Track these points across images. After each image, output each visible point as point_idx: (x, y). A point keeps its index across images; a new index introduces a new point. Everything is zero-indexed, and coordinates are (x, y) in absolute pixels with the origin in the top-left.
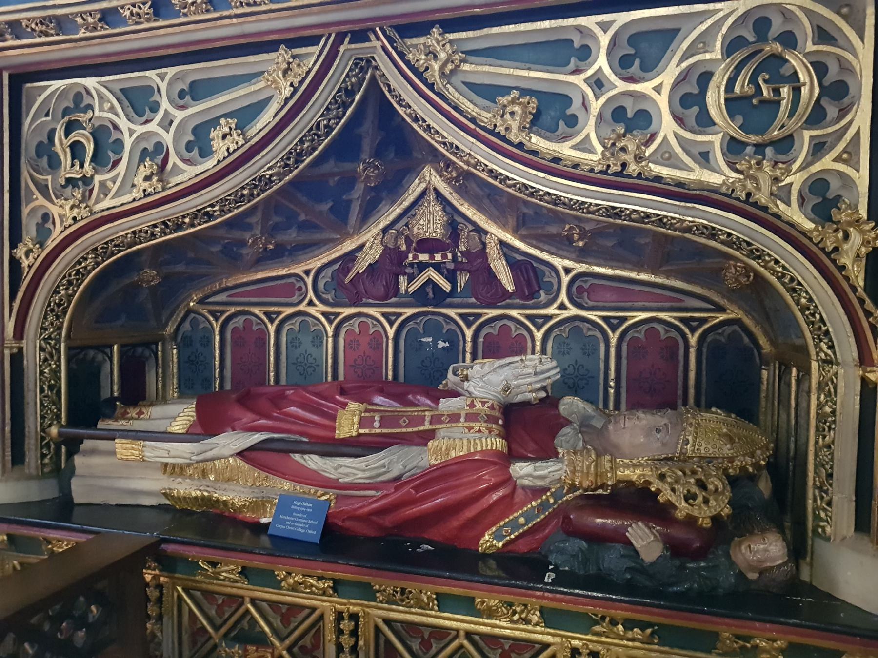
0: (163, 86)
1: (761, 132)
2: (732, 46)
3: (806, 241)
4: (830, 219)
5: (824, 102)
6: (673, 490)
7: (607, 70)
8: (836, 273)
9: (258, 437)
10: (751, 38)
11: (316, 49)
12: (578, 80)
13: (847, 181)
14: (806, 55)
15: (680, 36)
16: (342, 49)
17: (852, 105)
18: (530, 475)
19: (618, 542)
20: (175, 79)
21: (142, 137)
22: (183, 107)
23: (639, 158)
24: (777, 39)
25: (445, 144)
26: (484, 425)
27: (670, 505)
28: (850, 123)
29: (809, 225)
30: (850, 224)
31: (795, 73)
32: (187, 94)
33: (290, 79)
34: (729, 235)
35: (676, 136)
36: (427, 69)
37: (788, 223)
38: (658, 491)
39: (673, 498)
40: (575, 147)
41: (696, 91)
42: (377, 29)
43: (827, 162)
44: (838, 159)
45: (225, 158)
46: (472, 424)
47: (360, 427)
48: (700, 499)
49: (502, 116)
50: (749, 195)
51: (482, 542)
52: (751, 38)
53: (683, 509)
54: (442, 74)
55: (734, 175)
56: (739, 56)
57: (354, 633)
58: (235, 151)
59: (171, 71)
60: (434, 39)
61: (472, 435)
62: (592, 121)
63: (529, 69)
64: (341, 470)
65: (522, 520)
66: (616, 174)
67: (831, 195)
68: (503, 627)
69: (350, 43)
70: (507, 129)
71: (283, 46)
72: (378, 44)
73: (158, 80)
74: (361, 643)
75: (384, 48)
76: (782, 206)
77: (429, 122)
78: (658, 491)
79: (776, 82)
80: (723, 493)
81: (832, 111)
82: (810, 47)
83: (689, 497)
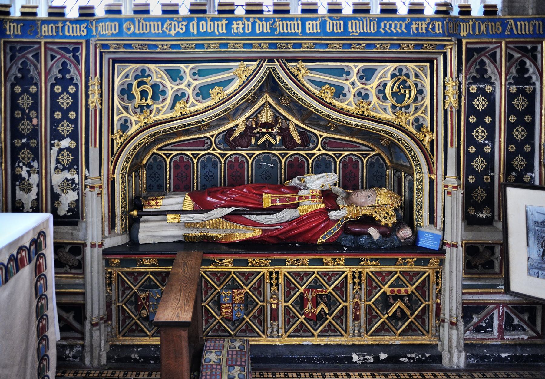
0: (187, 71)
1: (401, 103)
2: (393, 76)
3: (415, 137)
4: (420, 131)
5: (418, 95)
6: (380, 216)
7: (357, 81)
8: (423, 147)
9: (231, 210)
10: (398, 74)
11: (255, 64)
12: (348, 83)
13: (424, 119)
14: (413, 81)
15: (377, 71)
16: (264, 64)
17: (425, 97)
18: (336, 216)
19: (365, 235)
20: (193, 68)
21: (177, 90)
22: (196, 80)
23: (367, 110)
24: (404, 75)
25: (300, 99)
26: (318, 199)
27: (380, 221)
28: (425, 102)
29: (414, 132)
30: (426, 132)
31: (410, 86)
32: (197, 74)
33: (245, 73)
34: (392, 134)
35: (377, 103)
36: (298, 75)
37: (410, 132)
38: (376, 217)
39: (380, 219)
40: (347, 104)
41: (382, 89)
42: (280, 60)
43: (419, 114)
44: (422, 113)
45: (218, 102)
46: (314, 199)
47: (272, 203)
48: (388, 218)
49: (324, 93)
50: (399, 123)
51: (318, 240)
52: (398, 74)
53: (384, 222)
54: (303, 77)
55: (394, 116)
56: (394, 80)
57: (277, 279)
58: (222, 99)
59: (191, 65)
60: (301, 64)
61: (314, 203)
62: (352, 96)
63: (331, 77)
64: (266, 220)
65: (332, 231)
66: (361, 115)
67: (420, 123)
68: (330, 268)
69: (267, 62)
70: (326, 98)
71: (242, 62)
72: (278, 64)
73: (185, 68)
74: (280, 281)
75: (281, 65)
76: (408, 126)
77: (295, 91)
78: (376, 217)
79: (405, 88)
80: (394, 216)
81: (420, 98)
82: (414, 79)
83: (385, 218)
